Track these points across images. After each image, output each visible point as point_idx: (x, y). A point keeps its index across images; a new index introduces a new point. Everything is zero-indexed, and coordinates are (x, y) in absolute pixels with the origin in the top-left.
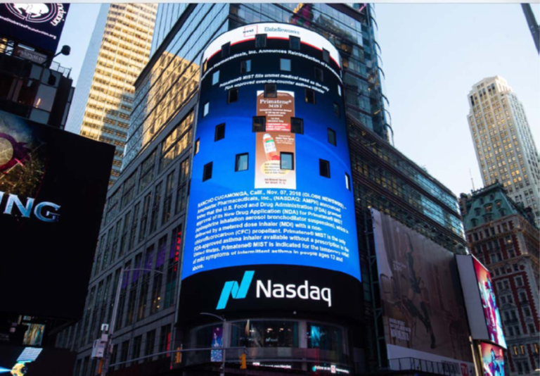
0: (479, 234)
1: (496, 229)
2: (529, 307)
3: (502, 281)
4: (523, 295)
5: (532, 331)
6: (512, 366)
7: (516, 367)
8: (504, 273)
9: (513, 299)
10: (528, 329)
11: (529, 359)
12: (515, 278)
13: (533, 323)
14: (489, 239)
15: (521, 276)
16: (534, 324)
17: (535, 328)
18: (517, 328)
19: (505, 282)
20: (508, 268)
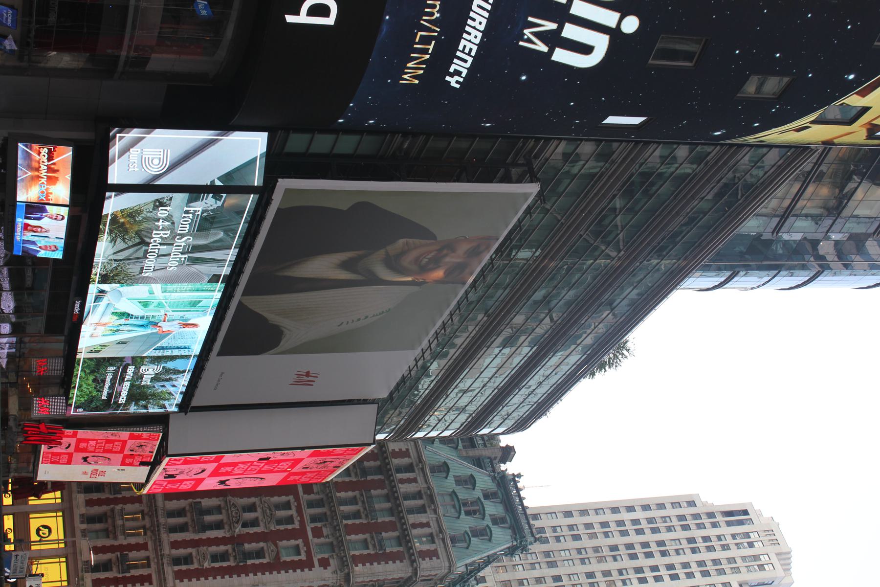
0: (410, 475)
1: (422, 518)
2: (232, 563)
3: (293, 512)
4: (259, 554)
5: (177, 561)
6: (99, 502)
7: (96, 510)
8: (314, 519)
9: (251, 530)
10: (182, 552)
11: (116, 543)
12: (300, 542)
13: (195, 566)
14: (397, 498)
15: (303, 557)
16: (192, 567)
17: (184, 567)
18: (183, 528)
19: (290, 520)
20: (325, 531)
